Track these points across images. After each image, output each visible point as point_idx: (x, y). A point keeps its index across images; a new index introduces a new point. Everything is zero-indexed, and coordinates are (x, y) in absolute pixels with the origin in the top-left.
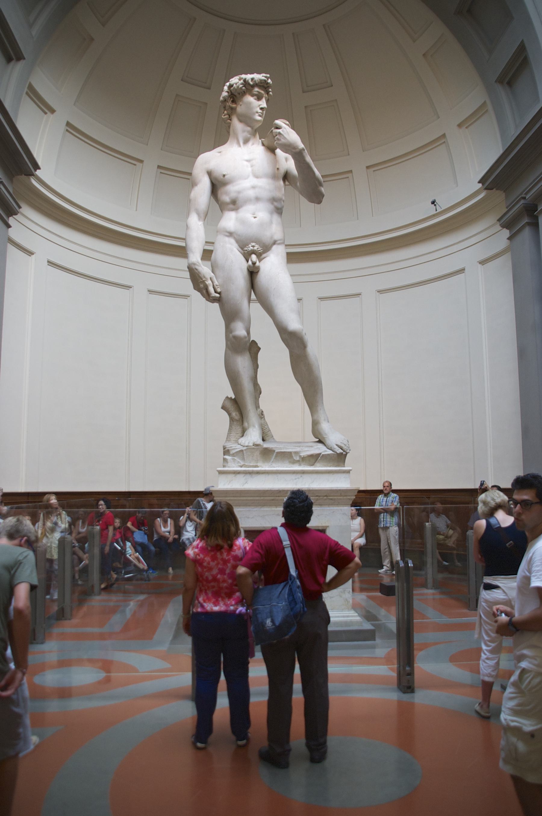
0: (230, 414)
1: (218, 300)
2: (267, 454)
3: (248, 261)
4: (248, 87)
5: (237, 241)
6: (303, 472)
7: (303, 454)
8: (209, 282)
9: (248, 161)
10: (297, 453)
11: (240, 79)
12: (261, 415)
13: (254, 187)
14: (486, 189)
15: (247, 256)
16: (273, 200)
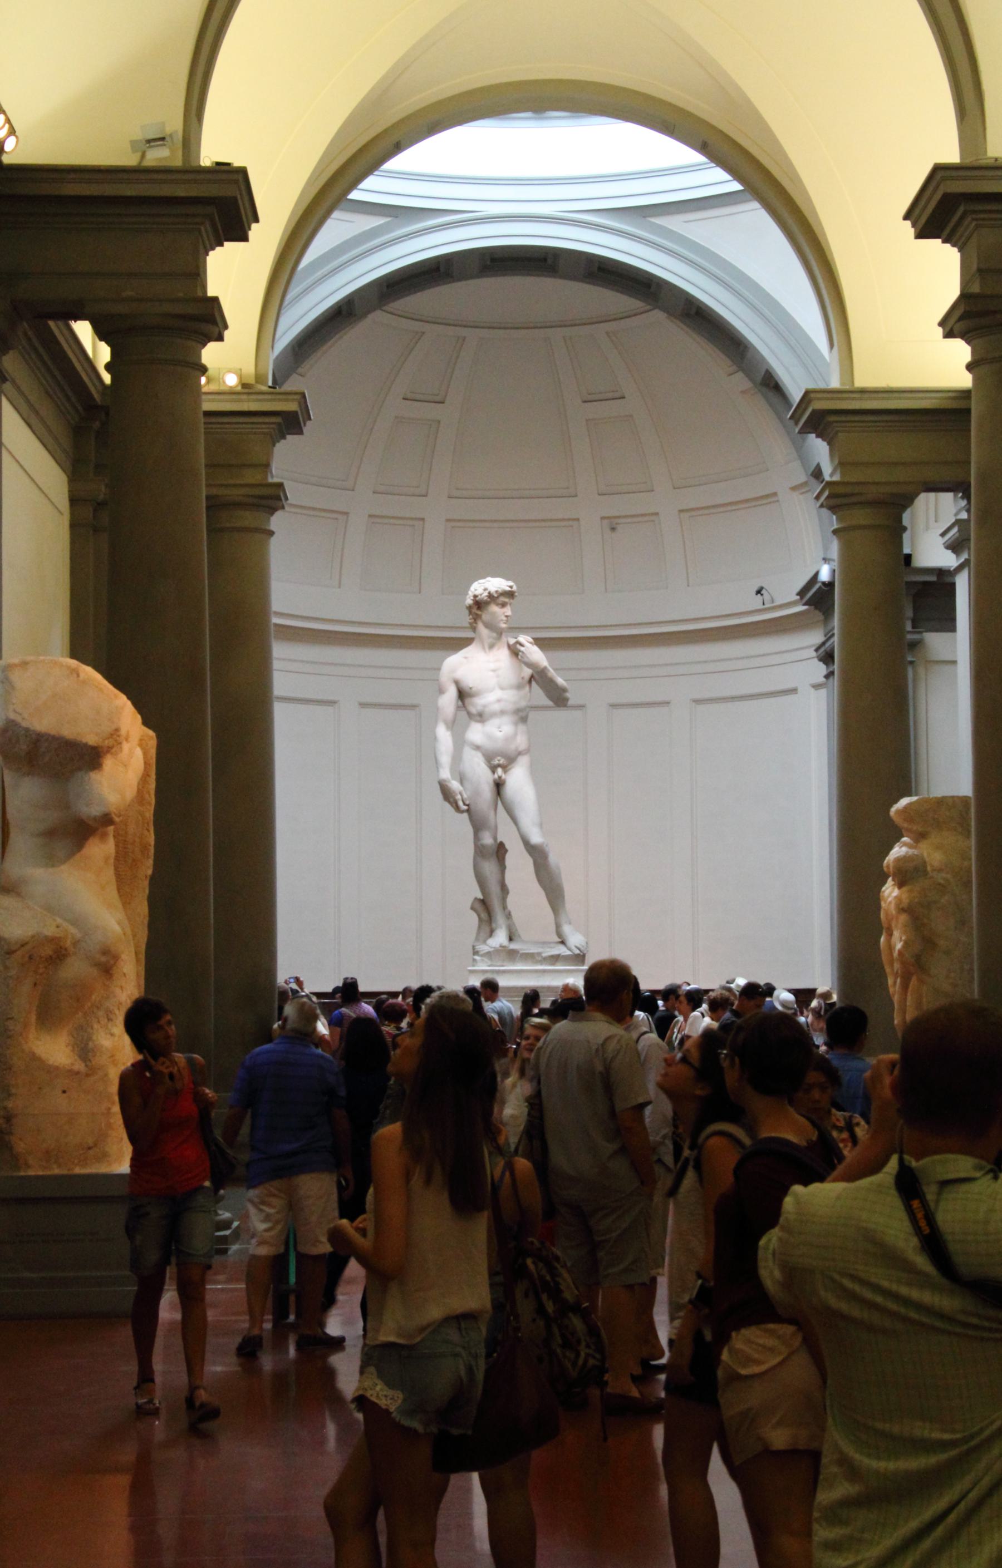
0: (479, 915)
1: (468, 811)
2: (512, 955)
3: (494, 772)
4: (493, 598)
5: (484, 755)
6: (544, 971)
7: (544, 955)
8: (459, 797)
9: (494, 671)
10: (539, 954)
11: (485, 590)
12: (509, 916)
13: (499, 701)
14: (804, 605)
15: (493, 769)
16: (517, 711)
